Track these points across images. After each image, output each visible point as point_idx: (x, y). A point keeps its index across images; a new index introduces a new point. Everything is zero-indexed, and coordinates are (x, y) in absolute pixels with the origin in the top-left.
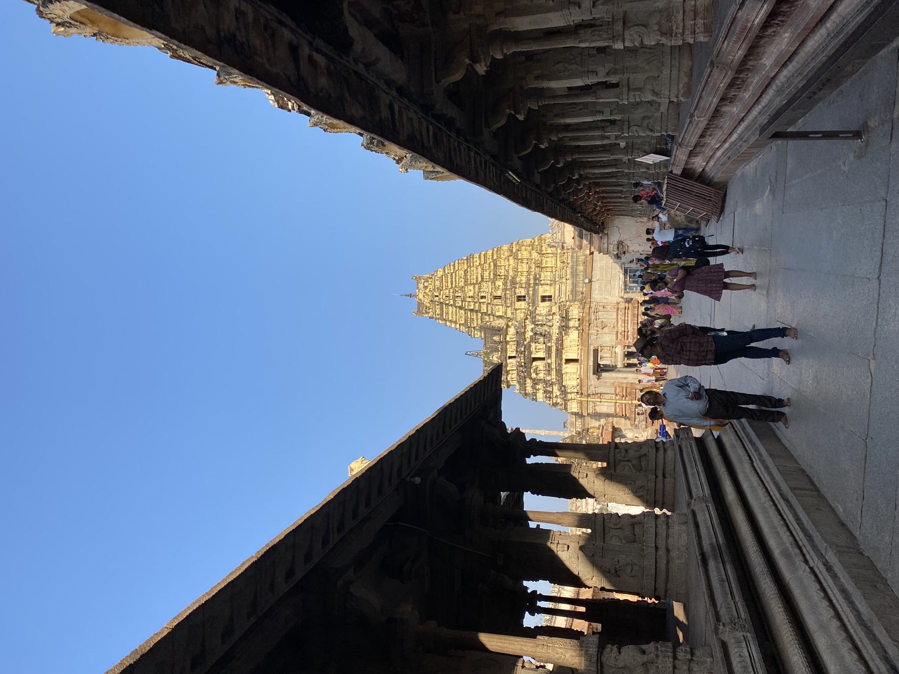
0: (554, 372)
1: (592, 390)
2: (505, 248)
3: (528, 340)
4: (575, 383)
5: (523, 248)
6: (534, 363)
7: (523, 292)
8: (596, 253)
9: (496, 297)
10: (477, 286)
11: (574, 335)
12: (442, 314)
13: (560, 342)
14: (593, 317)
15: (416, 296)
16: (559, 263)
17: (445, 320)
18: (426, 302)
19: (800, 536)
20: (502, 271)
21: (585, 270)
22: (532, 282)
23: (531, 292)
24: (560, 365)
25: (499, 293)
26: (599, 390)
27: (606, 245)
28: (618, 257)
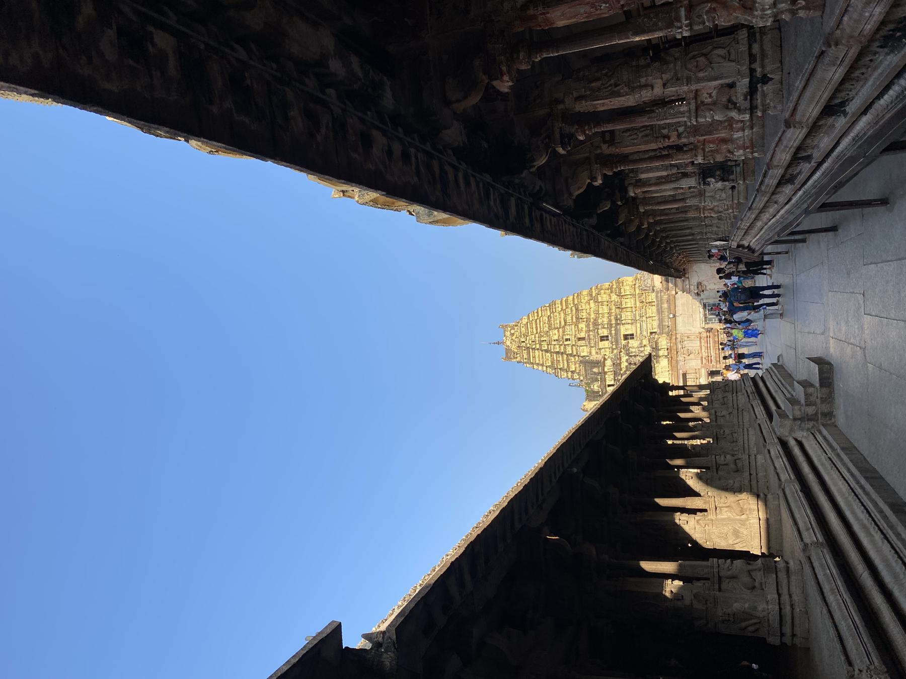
2: (585, 292)
3: (624, 370)
5: (602, 291)
7: (605, 332)
8: (680, 293)
9: (580, 339)
12: (529, 358)
14: (680, 346)
15: (503, 343)
16: (638, 304)
18: (514, 348)
19: (779, 383)
20: (584, 314)
21: (669, 308)
22: (613, 322)
23: (613, 332)
25: (582, 335)
28: (698, 294)
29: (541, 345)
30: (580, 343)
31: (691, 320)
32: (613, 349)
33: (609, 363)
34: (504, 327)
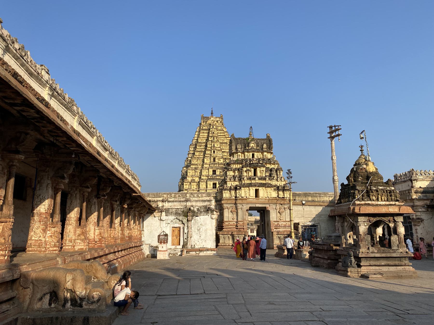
0: (249, 182)
1: (239, 206)
4: (243, 195)
6: (253, 170)
7: (218, 173)
10: (219, 149)
11: (274, 194)
12: (203, 130)
13: (270, 186)
14: (286, 206)
15: (212, 116)
17: (199, 132)
18: (209, 122)
21: (309, 201)
23: (218, 177)
24: (255, 186)
25: (217, 160)
26: (240, 211)
27: (420, 210)
29: (212, 137)
30: (212, 159)
31: (300, 216)
32: (208, 177)
33: (269, 156)
34: (221, 118)
